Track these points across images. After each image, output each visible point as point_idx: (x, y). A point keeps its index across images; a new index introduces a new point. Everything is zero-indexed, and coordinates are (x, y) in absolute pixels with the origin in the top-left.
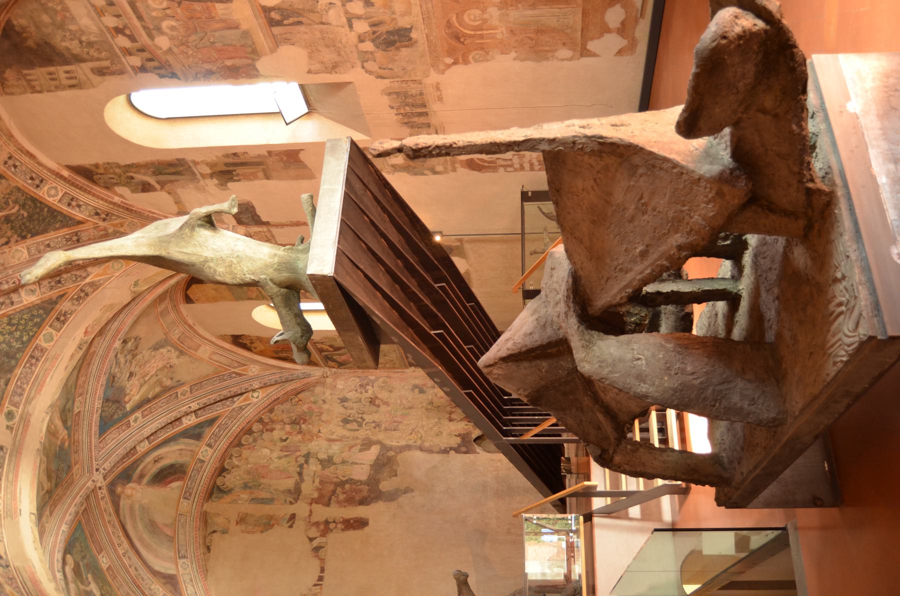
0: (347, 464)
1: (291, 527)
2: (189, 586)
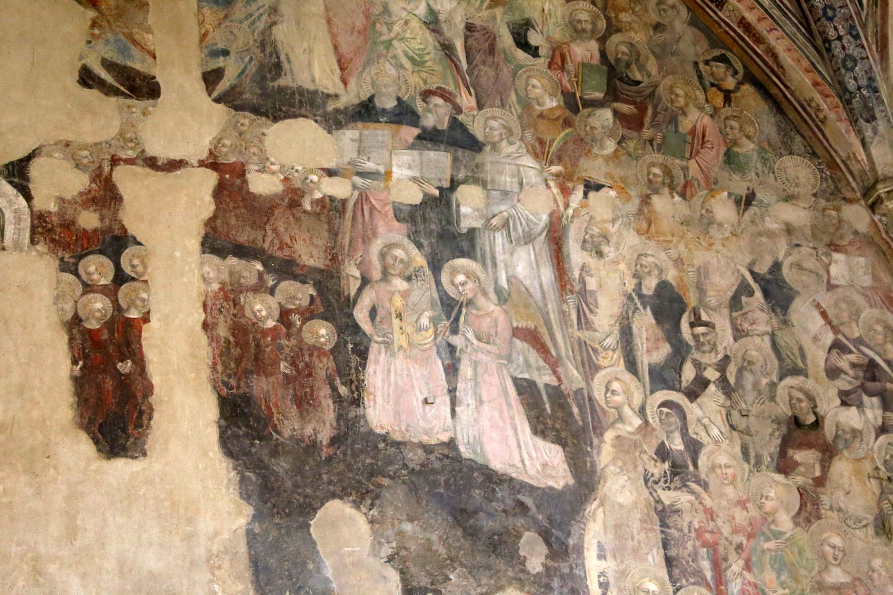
0: (445, 323)
1: (87, 78)
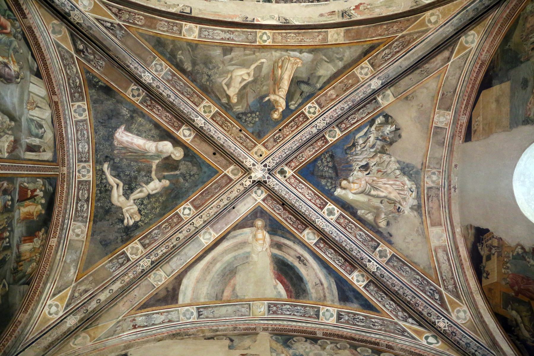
2: (163, 318)
